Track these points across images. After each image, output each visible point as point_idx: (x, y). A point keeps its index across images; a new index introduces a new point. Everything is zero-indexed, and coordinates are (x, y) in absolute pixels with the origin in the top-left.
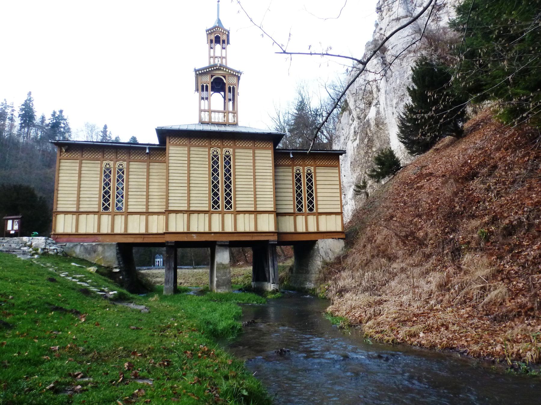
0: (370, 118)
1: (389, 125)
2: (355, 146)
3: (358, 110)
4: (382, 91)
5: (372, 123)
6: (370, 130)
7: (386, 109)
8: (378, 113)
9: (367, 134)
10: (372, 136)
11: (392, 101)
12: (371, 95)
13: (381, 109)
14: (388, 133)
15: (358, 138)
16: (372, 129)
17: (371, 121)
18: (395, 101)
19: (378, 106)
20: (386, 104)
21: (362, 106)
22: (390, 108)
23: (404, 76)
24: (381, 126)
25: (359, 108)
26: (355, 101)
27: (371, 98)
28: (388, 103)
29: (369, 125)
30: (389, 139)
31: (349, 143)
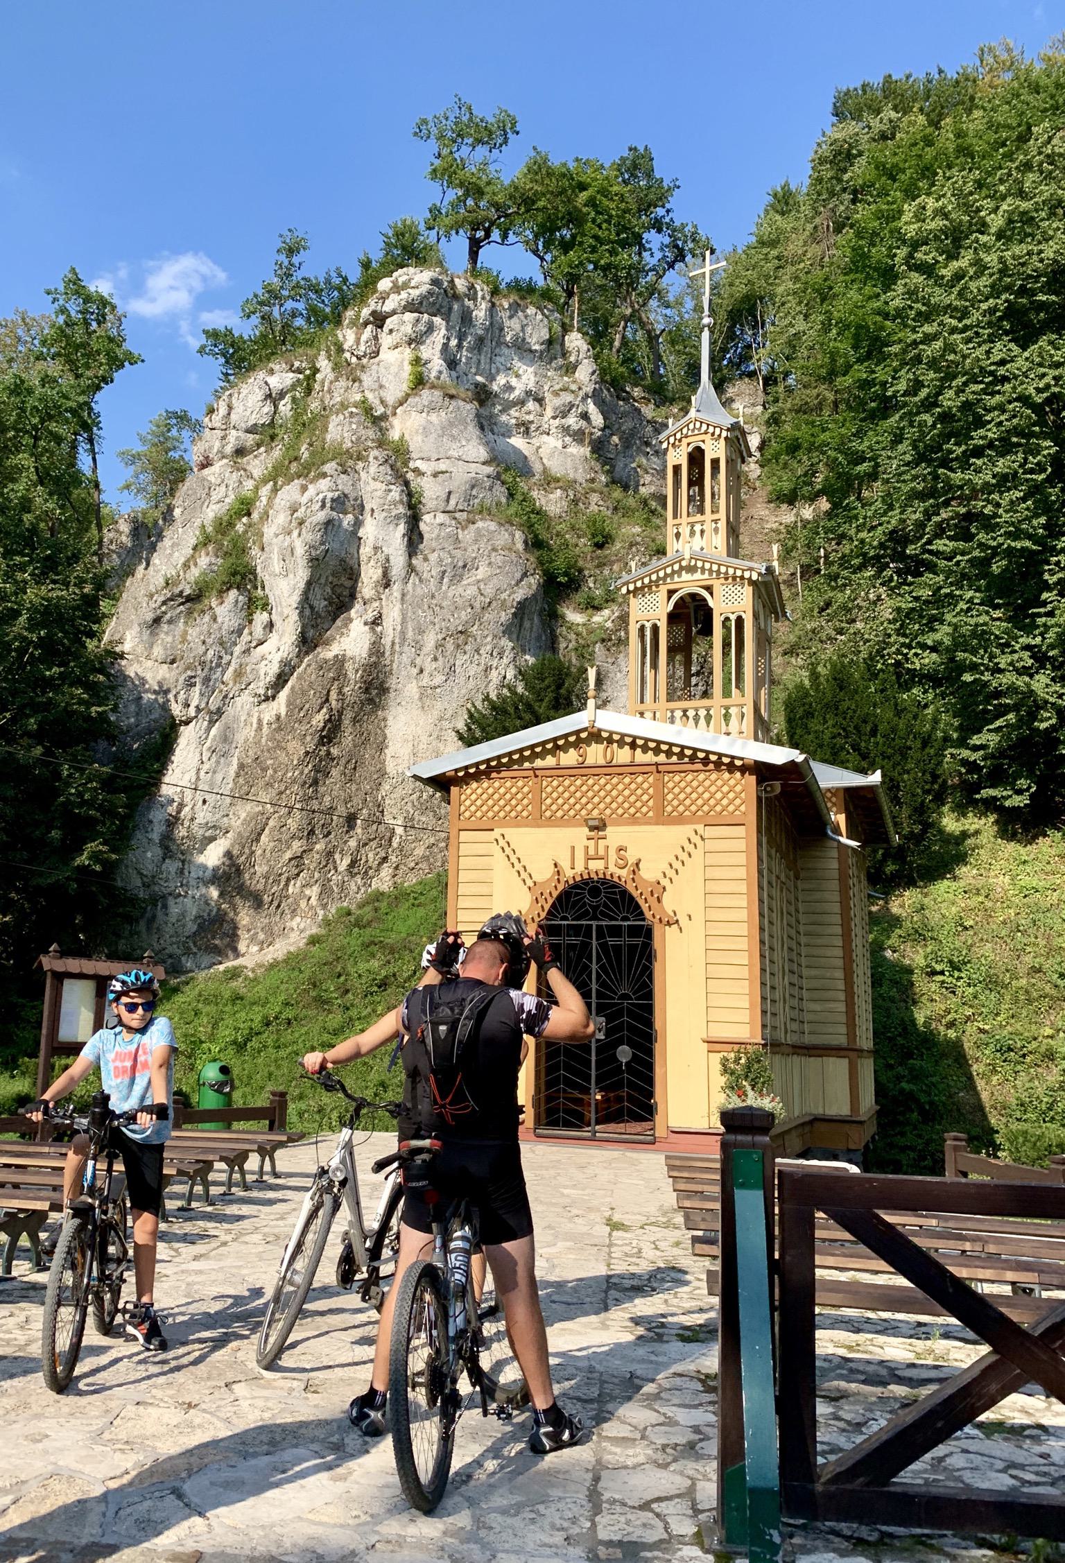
0: (349, 654)
1: (392, 695)
2: (267, 718)
3: (307, 612)
4: (396, 588)
5: (353, 675)
6: (340, 692)
7: (397, 647)
8: (376, 650)
9: (327, 700)
10: (340, 713)
11: (421, 632)
12: (348, 583)
13: (387, 641)
14: (385, 719)
15: (283, 695)
16: (346, 690)
17: (349, 667)
18: (430, 640)
19: (379, 629)
20: (403, 633)
21: (321, 604)
22: (409, 652)
23: (461, 576)
24: (374, 692)
25: (312, 607)
26: (309, 584)
27: (346, 593)
28: (410, 634)
29: (340, 675)
30: (385, 738)
31: (244, 702)
